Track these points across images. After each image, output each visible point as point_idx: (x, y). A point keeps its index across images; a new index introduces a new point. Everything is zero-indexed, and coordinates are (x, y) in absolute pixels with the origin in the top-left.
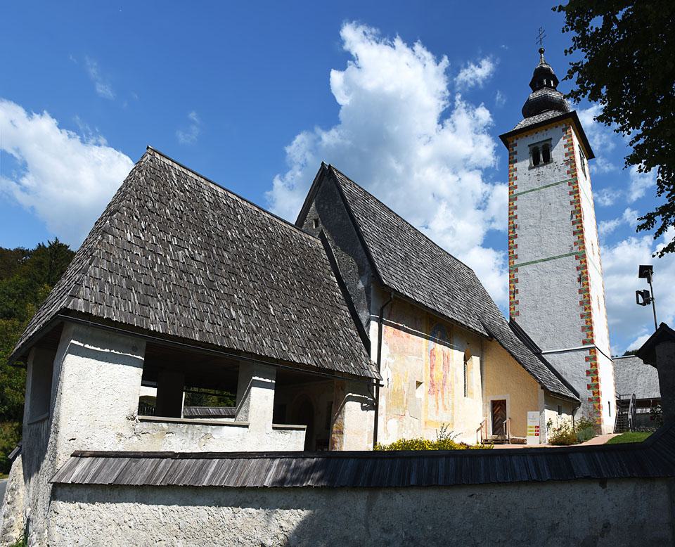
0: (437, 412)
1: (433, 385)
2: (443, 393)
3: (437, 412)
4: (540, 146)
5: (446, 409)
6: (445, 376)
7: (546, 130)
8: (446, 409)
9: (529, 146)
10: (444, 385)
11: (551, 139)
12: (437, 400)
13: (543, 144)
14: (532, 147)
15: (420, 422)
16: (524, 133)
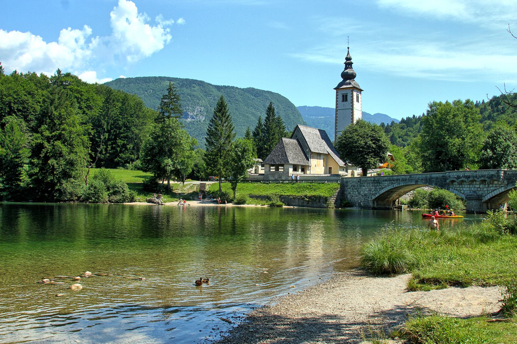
4: (345, 95)
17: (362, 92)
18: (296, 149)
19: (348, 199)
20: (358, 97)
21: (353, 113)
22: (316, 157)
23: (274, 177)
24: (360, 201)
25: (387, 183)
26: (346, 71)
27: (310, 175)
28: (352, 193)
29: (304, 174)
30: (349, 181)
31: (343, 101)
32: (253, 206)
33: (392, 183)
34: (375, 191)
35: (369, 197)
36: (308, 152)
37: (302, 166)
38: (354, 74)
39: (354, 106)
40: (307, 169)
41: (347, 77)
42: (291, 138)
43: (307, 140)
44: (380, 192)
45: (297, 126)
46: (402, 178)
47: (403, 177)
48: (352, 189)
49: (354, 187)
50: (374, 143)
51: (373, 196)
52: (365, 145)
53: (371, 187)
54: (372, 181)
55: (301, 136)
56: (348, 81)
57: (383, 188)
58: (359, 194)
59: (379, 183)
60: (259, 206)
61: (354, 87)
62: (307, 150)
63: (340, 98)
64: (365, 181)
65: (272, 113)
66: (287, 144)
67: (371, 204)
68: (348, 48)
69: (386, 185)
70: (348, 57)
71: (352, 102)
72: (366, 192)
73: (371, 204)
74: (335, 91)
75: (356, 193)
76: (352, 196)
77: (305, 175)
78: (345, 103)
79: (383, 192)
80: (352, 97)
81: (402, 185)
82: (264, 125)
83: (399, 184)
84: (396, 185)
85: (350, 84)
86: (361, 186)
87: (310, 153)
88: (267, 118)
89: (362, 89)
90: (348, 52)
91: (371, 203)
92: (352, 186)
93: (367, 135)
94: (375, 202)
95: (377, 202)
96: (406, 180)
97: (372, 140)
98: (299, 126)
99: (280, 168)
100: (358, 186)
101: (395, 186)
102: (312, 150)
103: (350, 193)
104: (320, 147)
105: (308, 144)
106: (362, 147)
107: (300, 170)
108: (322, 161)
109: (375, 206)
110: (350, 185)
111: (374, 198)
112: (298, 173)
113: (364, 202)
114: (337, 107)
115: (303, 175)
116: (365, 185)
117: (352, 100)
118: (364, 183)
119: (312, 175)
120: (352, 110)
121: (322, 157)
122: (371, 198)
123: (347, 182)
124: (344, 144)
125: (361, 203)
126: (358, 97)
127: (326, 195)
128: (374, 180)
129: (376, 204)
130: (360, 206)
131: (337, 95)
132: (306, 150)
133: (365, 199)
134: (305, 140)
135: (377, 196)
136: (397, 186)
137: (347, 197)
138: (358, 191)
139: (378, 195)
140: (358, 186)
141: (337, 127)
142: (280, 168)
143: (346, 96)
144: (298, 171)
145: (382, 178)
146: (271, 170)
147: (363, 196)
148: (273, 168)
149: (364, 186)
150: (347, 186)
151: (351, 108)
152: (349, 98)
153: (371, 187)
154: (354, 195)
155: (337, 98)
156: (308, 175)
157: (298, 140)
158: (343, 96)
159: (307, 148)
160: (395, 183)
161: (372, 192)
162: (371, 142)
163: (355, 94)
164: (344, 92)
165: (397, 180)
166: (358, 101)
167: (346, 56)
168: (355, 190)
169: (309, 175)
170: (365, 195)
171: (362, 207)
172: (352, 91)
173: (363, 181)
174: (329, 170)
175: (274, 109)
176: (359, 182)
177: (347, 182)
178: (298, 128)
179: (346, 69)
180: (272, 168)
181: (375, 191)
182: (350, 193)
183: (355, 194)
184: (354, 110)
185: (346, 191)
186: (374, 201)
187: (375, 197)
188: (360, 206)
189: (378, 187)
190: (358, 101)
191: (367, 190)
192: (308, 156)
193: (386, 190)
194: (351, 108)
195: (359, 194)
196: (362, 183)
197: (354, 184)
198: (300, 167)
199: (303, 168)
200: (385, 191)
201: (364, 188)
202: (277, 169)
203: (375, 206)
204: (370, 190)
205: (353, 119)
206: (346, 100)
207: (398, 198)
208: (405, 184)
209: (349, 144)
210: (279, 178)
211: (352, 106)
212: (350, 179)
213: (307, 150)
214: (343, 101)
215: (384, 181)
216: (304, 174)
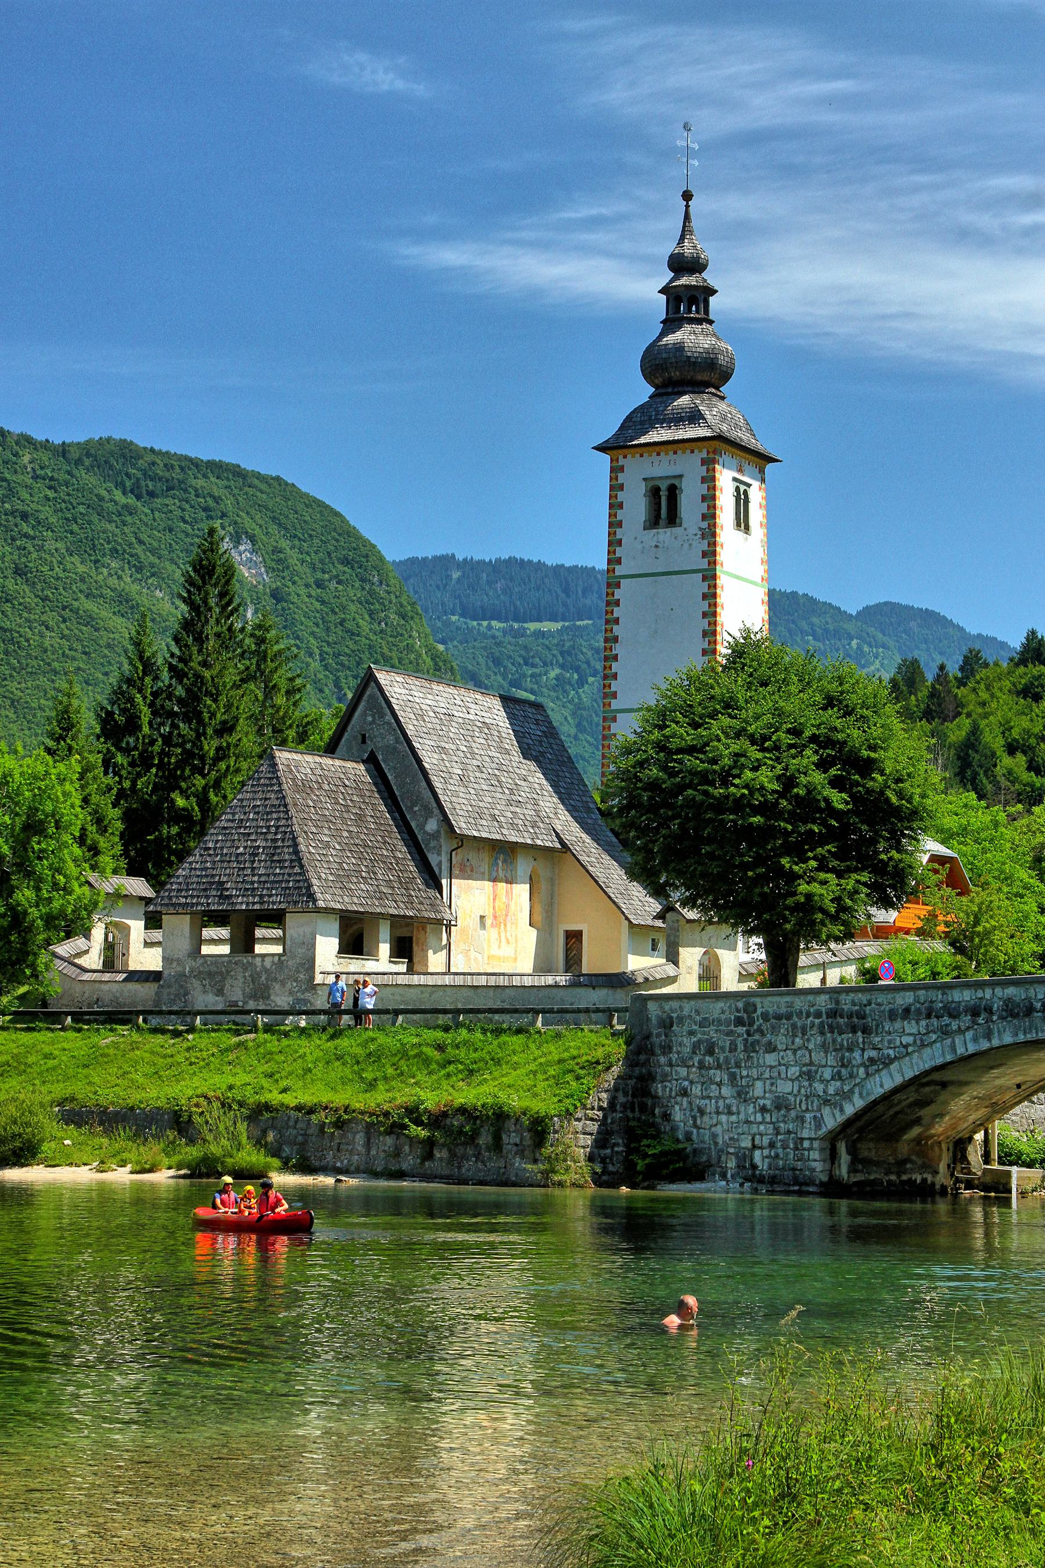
0: (499, 946)
1: (495, 917)
2: (505, 925)
3: (499, 946)
4: (664, 486)
5: (508, 942)
6: (508, 906)
7: (675, 453)
8: (508, 942)
9: (645, 479)
10: (507, 915)
11: (681, 476)
12: (499, 933)
13: (669, 482)
14: (651, 484)
15: (483, 957)
17: (770, 467)
18: (360, 818)
19: (674, 1129)
20: (742, 501)
21: (711, 596)
22: (485, 867)
23: (220, 992)
24: (746, 1143)
25: (911, 1027)
26: (670, 339)
27: (447, 980)
28: (696, 1090)
29: (410, 971)
30: (681, 1020)
31: (654, 522)
32: (81, 1176)
33: (945, 1032)
34: (837, 1076)
35: (801, 1119)
36: (435, 836)
37: (396, 921)
38: (722, 360)
40: (431, 939)
41: (676, 374)
42: (331, 749)
43: (430, 760)
44: (869, 1085)
45: (370, 678)
46: (1008, 1001)
47: (1011, 991)
48: (702, 1066)
49: (710, 1052)
50: (836, 783)
51: (826, 1111)
52: (782, 795)
53: (818, 1057)
54: (818, 1015)
55: (391, 739)
56: (684, 400)
57: (887, 1062)
58: (742, 1095)
59: (866, 1030)
60: (121, 1176)
61: (720, 438)
62: (432, 825)
63: (636, 507)
64: (778, 1017)
65: (222, 595)
66: (304, 787)
67: (816, 1164)
68: (687, 196)
69: (906, 1040)
70: (688, 250)
71: (710, 534)
72: (785, 1087)
73: (816, 1164)
74: (606, 458)
75: (726, 1091)
76: (702, 1112)
77: (416, 979)
78: (665, 535)
79: (889, 1085)
80: (710, 499)
81: (1008, 1039)
82: (172, 668)
83: (988, 1036)
84: (967, 1045)
85: (694, 417)
86: (751, 1048)
87: (446, 846)
88: (187, 625)
90: (687, 217)
91: (815, 1155)
92: (695, 1047)
93: (796, 732)
94: (842, 1148)
95: (852, 1151)
96: (1030, 1010)
97: (823, 765)
98: (382, 677)
99: (259, 933)
100: (733, 1049)
101: (960, 1051)
102: (462, 825)
103: (684, 1093)
104: (509, 803)
105: (438, 784)
106: (765, 809)
107: (385, 949)
108: (522, 891)
109: (843, 1171)
110: (688, 1042)
111: (832, 1120)
112: (370, 966)
113: (772, 1145)
114: (614, 561)
115: (401, 980)
116: (780, 1041)
117: (710, 516)
118: (774, 1030)
119: (459, 981)
120: (710, 577)
121: (523, 866)
122: (818, 1122)
123: (667, 1024)
124: (653, 786)
125: (757, 1154)
126: (742, 501)
127: (539, 1106)
128: (833, 1014)
129: (845, 1158)
130: (750, 1175)
131: (616, 488)
132: (422, 826)
133: (778, 1132)
134: (419, 761)
135: (850, 1110)
136: (972, 1049)
137: (667, 1117)
138: (733, 1077)
139: (859, 1103)
140: (733, 1049)
141: (615, 686)
142: (259, 933)
143: (673, 491)
144: (373, 954)
145: (881, 998)
146: (206, 950)
147: (763, 1109)
148: (224, 932)
149: (771, 1048)
150: (667, 1049)
151: (704, 564)
152: (689, 506)
153: (818, 1057)
154: (710, 1106)
155: (615, 506)
156: (430, 980)
157: (372, 762)
158: (654, 493)
159: (428, 813)
160: (960, 1031)
161: (819, 1087)
162: (818, 777)
163: (725, 479)
164: (661, 468)
165: (975, 1012)
166: (742, 522)
167: (670, 248)
168: (717, 1075)
169: (439, 981)
170: (781, 1104)
171: (761, 1180)
172: (709, 463)
173: (765, 1016)
174: (567, 951)
175: (230, 572)
176: (739, 1022)
177: (667, 1024)
178: (372, 689)
179: (671, 323)
180: (208, 933)
181: (837, 1076)
182: (684, 1093)
183: (720, 1097)
184: (722, 580)
185: (665, 1077)
186: (832, 1139)
187: (840, 1119)
188: (750, 1175)
189: (857, 1054)
190: (742, 522)
191: (794, 1071)
192: (433, 859)
193: (909, 1074)
194: (704, 564)
195: (742, 1095)
196: (760, 1031)
197: (712, 1033)
198: (385, 931)
199: (404, 933)
200: (898, 1080)
201: (771, 1059)
202: (244, 943)
203: (843, 1171)
204: (810, 1076)
205: (710, 633)
206: (673, 519)
207: (983, 1124)
208: (1021, 1038)
209: (681, 788)
210: (254, 997)
211: (710, 554)
212: (688, 1007)
213: (432, 825)
214: (654, 522)
215: (892, 1016)
216: (410, 971)
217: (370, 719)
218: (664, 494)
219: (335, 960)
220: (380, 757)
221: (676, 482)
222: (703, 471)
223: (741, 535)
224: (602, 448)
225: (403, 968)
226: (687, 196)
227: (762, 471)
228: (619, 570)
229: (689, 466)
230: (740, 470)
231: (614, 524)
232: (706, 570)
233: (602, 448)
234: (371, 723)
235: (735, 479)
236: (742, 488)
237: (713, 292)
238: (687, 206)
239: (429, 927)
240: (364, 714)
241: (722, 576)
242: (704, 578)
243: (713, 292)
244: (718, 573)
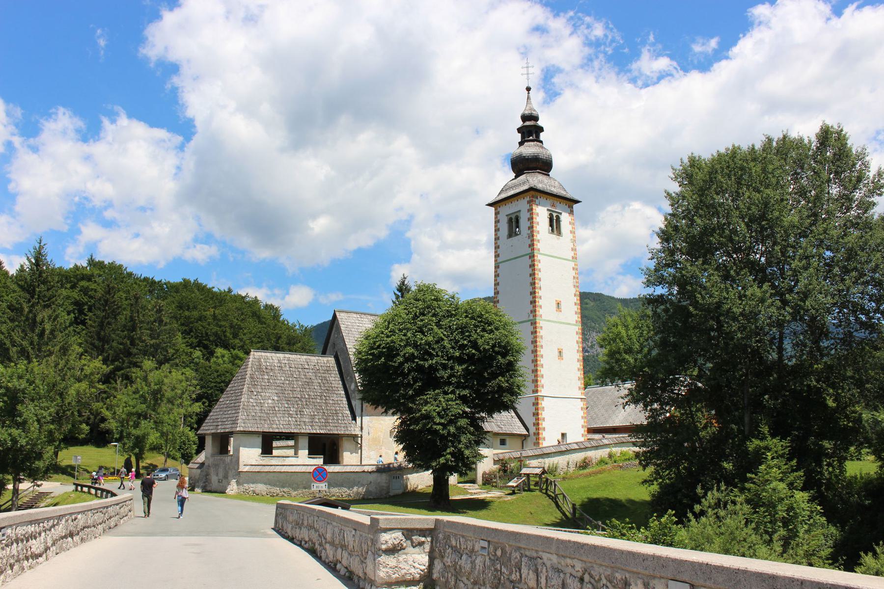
4: (513, 217)
9: (507, 215)
11: (520, 211)
13: (516, 214)
14: (509, 217)
16: (504, 202)
17: (575, 206)
31: (512, 234)
39: (538, 245)
62: (353, 386)
68: (528, 89)
71: (531, 236)
74: (493, 209)
89: (576, 198)
117: (531, 228)
120: (532, 256)
131: (497, 222)
132: (350, 386)
142: (275, 444)
151: (529, 250)
152: (524, 223)
158: (510, 221)
184: (539, 257)
192: (353, 403)
217: (336, 336)
218: (513, 220)
219: (259, 458)
220: (339, 354)
221: (518, 214)
222: (528, 206)
223: (554, 236)
224: (490, 205)
225: (319, 461)
226: (528, 89)
227: (571, 207)
228: (499, 260)
229: (521, 205)
230: (553, 206)
231: (497, 239)
232: (530, 253)
233: (490, 205)
234: (337, 337)
235: (548, 210)
236: (555, 215)
237: (541, 129)
238: (529, 93)
239: (344, 438)
240: (335, 334)
241: (539, 255)
242: (530, 257)
243: (541, 129)
244: (535, 254)
